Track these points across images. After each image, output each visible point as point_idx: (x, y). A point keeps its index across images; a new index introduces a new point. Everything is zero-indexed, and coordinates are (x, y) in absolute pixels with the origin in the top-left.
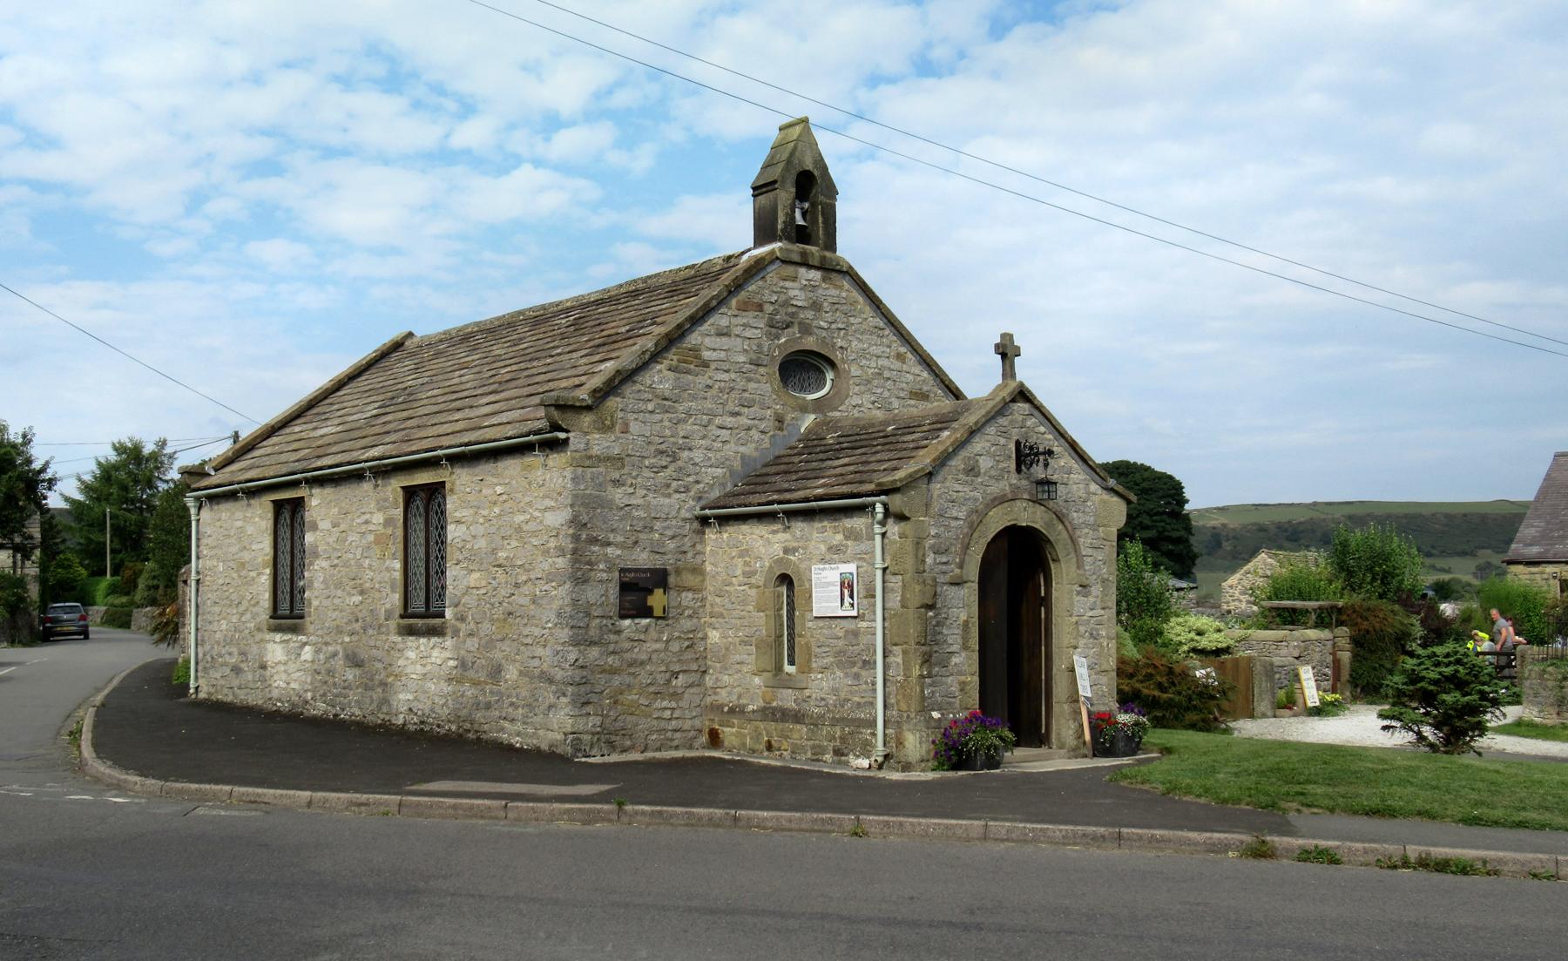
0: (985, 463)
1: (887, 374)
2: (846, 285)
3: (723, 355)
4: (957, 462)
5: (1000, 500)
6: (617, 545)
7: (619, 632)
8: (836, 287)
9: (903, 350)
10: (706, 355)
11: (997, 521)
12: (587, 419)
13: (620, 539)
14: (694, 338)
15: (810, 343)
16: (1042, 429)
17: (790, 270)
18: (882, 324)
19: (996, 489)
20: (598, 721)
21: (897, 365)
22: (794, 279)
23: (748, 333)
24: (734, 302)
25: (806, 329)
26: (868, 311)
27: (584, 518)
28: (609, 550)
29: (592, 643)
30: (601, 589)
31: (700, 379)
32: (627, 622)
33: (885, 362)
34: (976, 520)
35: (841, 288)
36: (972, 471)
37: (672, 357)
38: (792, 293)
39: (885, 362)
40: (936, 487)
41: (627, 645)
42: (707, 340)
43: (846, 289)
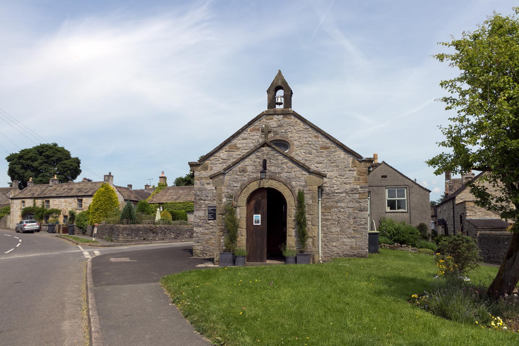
0: (250, 169)
1: (310, 143)
2: (293, 117)
3: (245, 145)
4: (236, 168)
5: (255, 179)
6: (208, 200)
7: (208, 224)
8: (288, 119)
9: (316, 134)
10: (238, 145)
11: (254, 186)
12: (199, 168)
13: (209, 199)
14: (234, 141)
15: (278, 137)
16: (277, 155)
17: (270, 117)
18: (308, 127)
19: (255, 175)
20: (202, 247)
21: (314, 139)
22: (272, 119)
23: (254, 138)
24: (249, 129)
25: (276, 133)
26: (302, 124)
27: (198, 193)
28: (206, 202)
29: (200, 226)
30: (203, 212)
31: (236, 153)
32: (211, 221)
33: (310, 139)
34: (244, 187)
35: (291, 119)
36: (244, 171)
37: (227, 147)
38: (271, 124)
39: (310, 139)
40: (227, 177)
41: (211, 227)
42: (239, 142)
43: (293, 119)
